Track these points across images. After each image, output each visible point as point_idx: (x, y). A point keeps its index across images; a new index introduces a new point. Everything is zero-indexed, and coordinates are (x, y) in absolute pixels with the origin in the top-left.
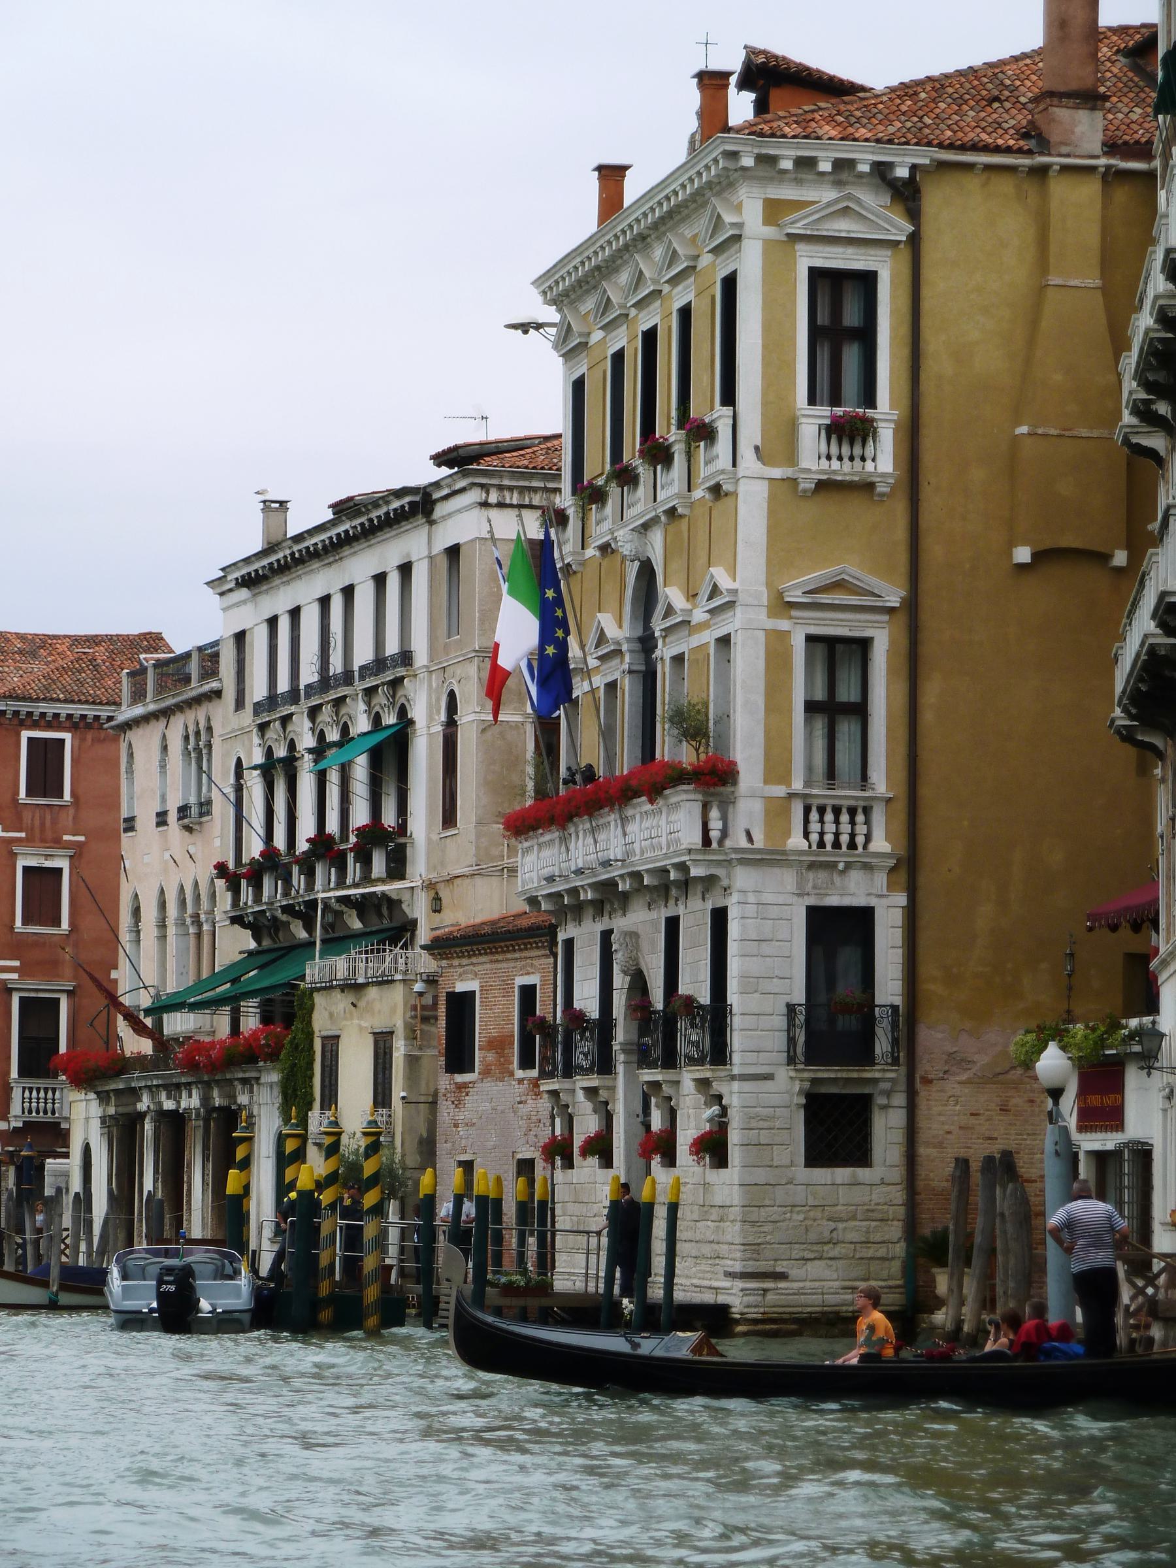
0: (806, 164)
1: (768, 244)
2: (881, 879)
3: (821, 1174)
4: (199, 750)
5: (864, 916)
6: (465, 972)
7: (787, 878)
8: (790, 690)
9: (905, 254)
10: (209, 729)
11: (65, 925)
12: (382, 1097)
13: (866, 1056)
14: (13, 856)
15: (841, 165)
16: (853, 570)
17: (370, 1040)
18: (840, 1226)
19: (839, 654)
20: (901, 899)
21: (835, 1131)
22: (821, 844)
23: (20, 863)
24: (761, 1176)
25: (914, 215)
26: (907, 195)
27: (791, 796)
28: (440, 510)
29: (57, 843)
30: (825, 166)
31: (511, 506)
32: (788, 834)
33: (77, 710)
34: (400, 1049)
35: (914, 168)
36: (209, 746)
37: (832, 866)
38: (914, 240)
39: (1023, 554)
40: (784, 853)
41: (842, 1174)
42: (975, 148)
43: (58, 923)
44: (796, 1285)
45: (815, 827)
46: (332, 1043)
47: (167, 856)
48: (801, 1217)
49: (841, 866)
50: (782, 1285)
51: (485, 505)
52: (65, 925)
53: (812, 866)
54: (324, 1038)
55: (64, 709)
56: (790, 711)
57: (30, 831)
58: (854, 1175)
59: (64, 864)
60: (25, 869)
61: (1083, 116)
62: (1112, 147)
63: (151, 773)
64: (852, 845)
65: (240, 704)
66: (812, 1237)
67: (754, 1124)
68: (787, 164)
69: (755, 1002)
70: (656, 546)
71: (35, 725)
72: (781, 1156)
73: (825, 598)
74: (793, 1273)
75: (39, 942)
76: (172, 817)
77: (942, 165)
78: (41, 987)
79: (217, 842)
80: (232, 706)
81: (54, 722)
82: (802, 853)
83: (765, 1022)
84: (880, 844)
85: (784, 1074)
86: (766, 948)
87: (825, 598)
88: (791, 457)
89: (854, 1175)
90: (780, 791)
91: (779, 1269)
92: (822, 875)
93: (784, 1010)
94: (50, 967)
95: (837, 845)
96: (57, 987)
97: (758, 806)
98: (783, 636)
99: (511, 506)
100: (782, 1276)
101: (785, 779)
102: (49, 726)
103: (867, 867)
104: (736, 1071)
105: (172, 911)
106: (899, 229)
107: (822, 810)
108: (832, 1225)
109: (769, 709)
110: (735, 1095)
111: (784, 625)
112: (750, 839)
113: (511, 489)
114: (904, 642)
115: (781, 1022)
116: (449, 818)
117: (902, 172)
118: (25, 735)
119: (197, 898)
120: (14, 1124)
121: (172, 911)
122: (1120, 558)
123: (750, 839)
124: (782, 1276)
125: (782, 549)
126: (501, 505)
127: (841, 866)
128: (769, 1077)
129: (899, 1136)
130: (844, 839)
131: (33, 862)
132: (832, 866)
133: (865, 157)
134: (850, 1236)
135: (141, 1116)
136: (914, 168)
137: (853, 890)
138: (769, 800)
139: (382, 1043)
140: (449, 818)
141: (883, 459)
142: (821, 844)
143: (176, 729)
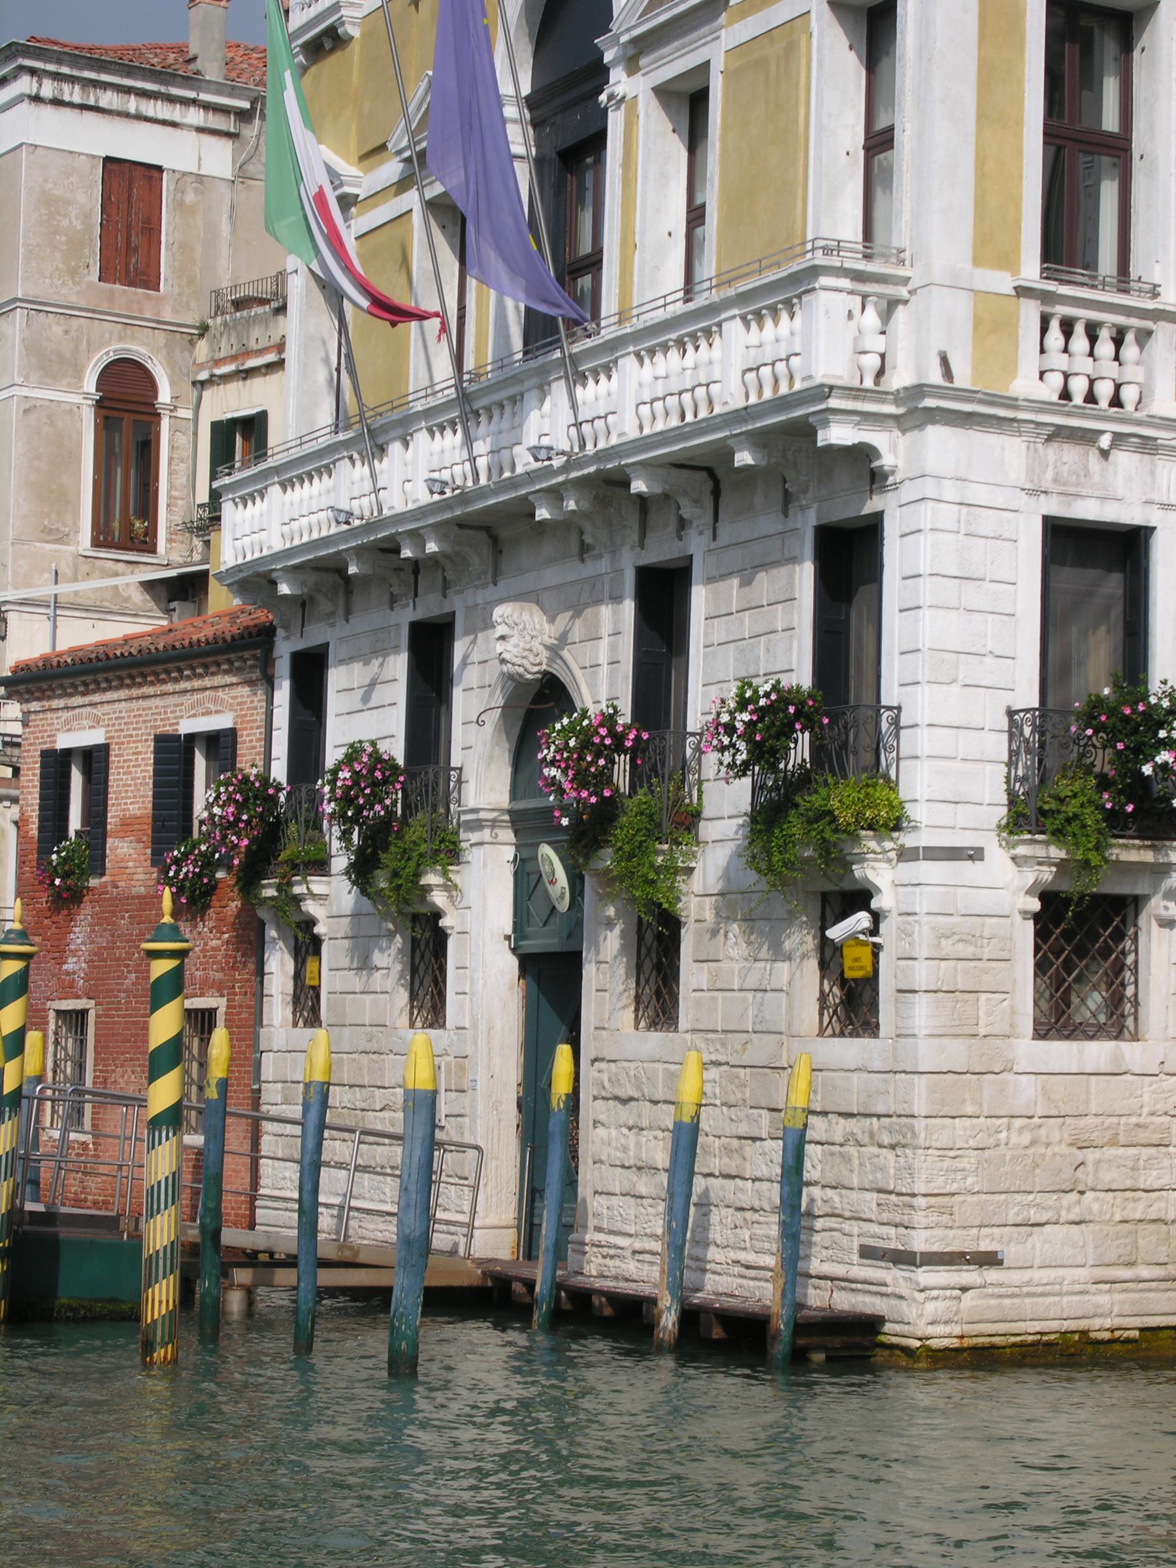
6: (77, 718)
7: (1009, 454)
8: (1020, 82)
18: (1091, 1156)
22: (1066, 395)
27: (1022, 292)
31: (71, 105)
32: (1011, 370)
37: (1087, 437)
40: (1011, 403)
44: (1016, 1277)
48: (1026, 1138)
49: (1105, 441)
50: (992, 1275)
53: (1059, 434)
56: (1019, 123)
58: (1117, 1057)
64: (1116, 402)
66: (1041, 1179)
67: (948, 948)
72: (987, 1013)
74: (1010, 1254)
82: (1044, 406)
83: (967, 744)
86: (974, 595)
89: (1117, 1057)
91: (985, 1246)
92: (1069, 453)
93: (1004, 723)
95: (1091, 398)
97: (961, 307)
99: (71, 105)
100: (990, 1260)
101: (1009, 261)
107: (1067, 327)
108: (1080, 1155)
109: (982, 117)
112: (948, 373)
113: (72, 80)
115: (1000, 747)
123: (948, 373)
124: (990, 1260)
126: (57, 102)
127: (1105, 441)
128: (975, 855)
130: (1104, 390)
132: (1087, 437)
134: (1108, 1177)
142: (1066, 395)
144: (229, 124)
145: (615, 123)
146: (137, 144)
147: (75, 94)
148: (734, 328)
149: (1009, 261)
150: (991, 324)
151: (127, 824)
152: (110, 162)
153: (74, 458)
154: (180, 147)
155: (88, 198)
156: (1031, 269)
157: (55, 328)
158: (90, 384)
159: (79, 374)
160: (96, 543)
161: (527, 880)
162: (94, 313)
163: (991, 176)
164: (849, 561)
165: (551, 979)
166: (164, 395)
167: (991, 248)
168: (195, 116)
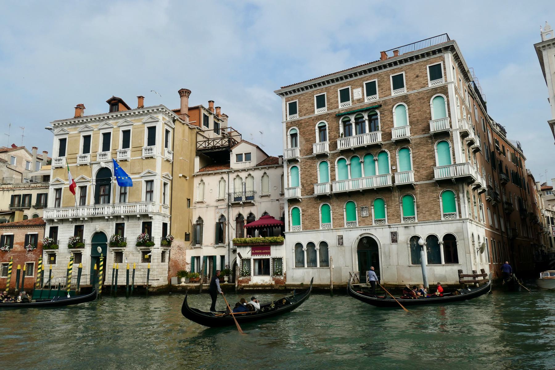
5: (167, 224)
39: (181, 175)
85: (160, 248)
117: (176, 118)
151: (17, 243)
161: (94, 250)
167: (161, 203)
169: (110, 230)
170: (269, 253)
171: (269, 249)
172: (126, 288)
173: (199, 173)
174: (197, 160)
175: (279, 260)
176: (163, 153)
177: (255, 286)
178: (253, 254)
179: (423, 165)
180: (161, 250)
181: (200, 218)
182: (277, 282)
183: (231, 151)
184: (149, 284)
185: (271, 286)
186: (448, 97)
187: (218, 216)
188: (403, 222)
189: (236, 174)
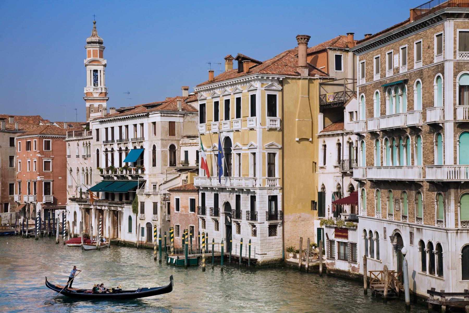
0: (268, 78)
1: (262, 90)
2: (278, 191)
3: (271, 237)
4: (88, 146)
7: (266, 191)
9: (281, 93)
10: (90, 144)
11: (51, 170)
12: (155, 212)
13: (277, 219)
14: (42, 160)
15: (273, 78)
16: (275, 143)
17: (153, 204)
19: (271, 156)
20: (281, 194)
21: (272, 230)
23: (44, 161)
24: (263, 239)
25: (282, 86)
26: (281, 83)
28: (150, 116)
29: (50, 157)
30: (270, 78)
32: (265, 184)
33: (52, 136)
34: (159, 206)
35: (283, 79)
36: (90, 146)
38: (282, 90)
41: (274, 237)
42: (290, 75)
43: (50, 170)
45: (269, 183)
46: (143, 204)
47: (79, 162)
51: (161, 116)
52: (51, 170)
53: (269, 189)
54: (141, 202)
55: (50, 136)
57: (45, 155)
59: (51, 160)
60: (45, 162)
61: (305, 70)
62: (309, 75)
63: (74, 148)
65: (98, 140)
68: (265, 78)
69: (262, 211)
70: (231, 136)
71: (46, 138)
73: (271, 147)
75: (47, 173)
76: (81, 156)
77: (286, 78)
78: (47, 180)
79: (92, 162)
80: (96, 140)
81: (49, 138)
84: (278, 185)
87: (271, 147)
88: (265, 125)
90: (265, 178)
92: (270, 190)
94: (49, 177)
96: (50, 180)
97: (261, 180)
98: (264, 153)
100: (266, 254)
101: (265, 176)
102: (48, 138)
103: (277, 189)
104: (258, 222)
105: (81, 171)
106: (280, 88)
110: (258, 225)
111: (265, 151)
114: (281, 154)
115: (265, 214)
116: (154, 165)
117: (281, 79)
118: (44, 140)
119: (87, 170)
120: (44, 202)
121: (81, 171)
122: (311, 140)
124: (266, 254)
125: (264, 139)
126: (164, 116)
129: (282, 231)
131: (46, 160)
132: (272, 189)
133: (276, 77)
135: (91, 209)
136: (283, 79)
137: (274, 193)
138: (263, 179)
139: (155, 205)
140: (154, 165)
141: (278, 125)
143: (81, 143)
144: (182, 116)
145: (232, 155)
146: (172, 119)
147: (166, 115)
148: (243, 180)
149: (265, 176)
150: (264, 181)
152: (170, 122)
153: (167, 156)
154: (177, 119)
155: (167, 126)
156: (267, 177)
157: (165, 142)
158: (168, 148)
159: (167, 146)
160: (170, 166)
161: (226, 219)
162: (169, 140)
163: (264, 170)
164: (253, 199)
165: (229, 228)
166: (176, 148)
167: (264, 175)
168: (178, 115)
169: (233, 201)
170: (346, 237)
171: (347, 233)
172: (238, 261)
173: (322, 134)
174: (320, 117)
175: (354, 245)
176: (263, 123)
177: (338, 271)
178: (336, 236)
179: (428, 159)
180: (267, 224)
181: (323, 185)
182: (354, 268)
183: (344, 108)
184: (256, 258)
185: (349, 272)
186: (444, 78)
187: (336, 184)
188: (416, 222)
189: (348, 136)
